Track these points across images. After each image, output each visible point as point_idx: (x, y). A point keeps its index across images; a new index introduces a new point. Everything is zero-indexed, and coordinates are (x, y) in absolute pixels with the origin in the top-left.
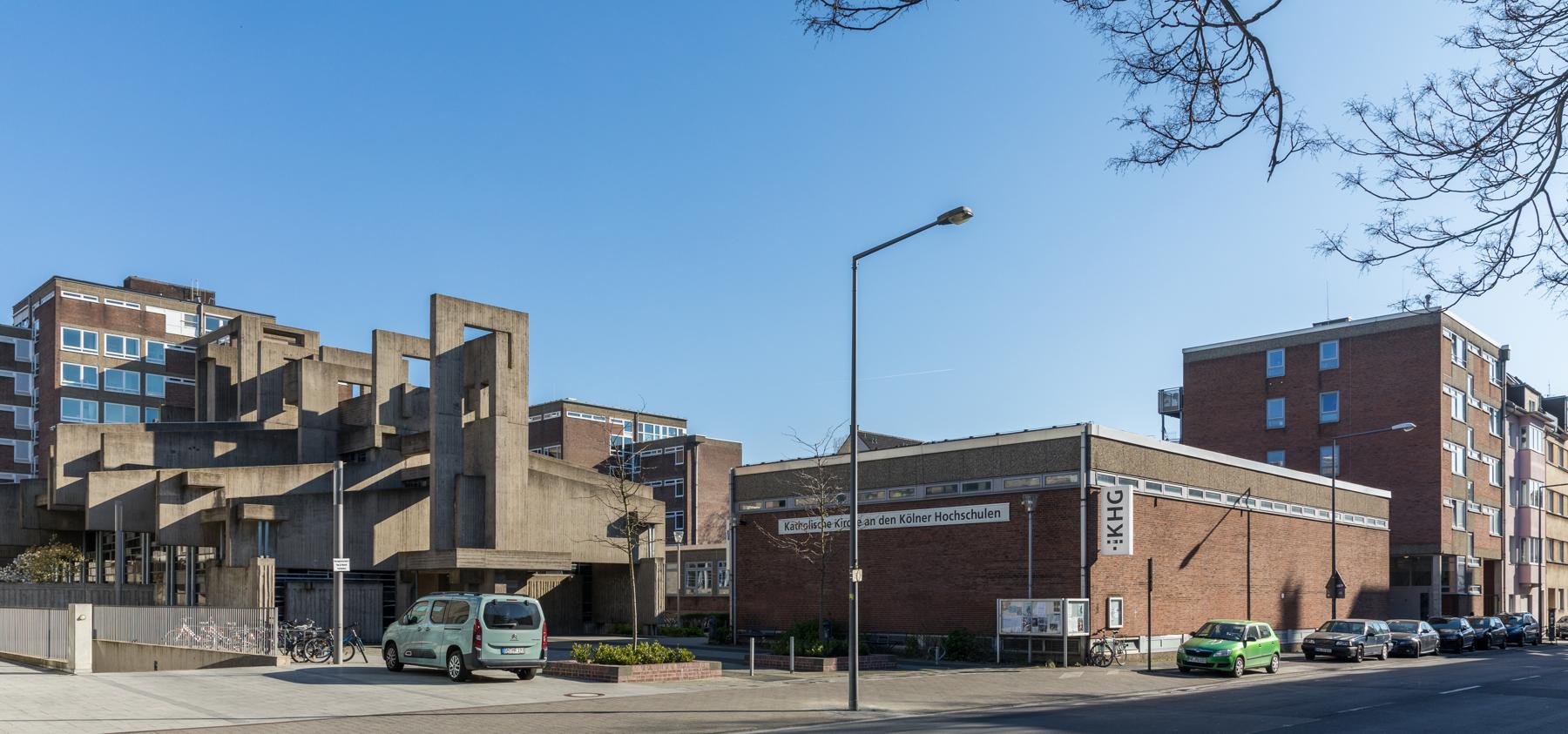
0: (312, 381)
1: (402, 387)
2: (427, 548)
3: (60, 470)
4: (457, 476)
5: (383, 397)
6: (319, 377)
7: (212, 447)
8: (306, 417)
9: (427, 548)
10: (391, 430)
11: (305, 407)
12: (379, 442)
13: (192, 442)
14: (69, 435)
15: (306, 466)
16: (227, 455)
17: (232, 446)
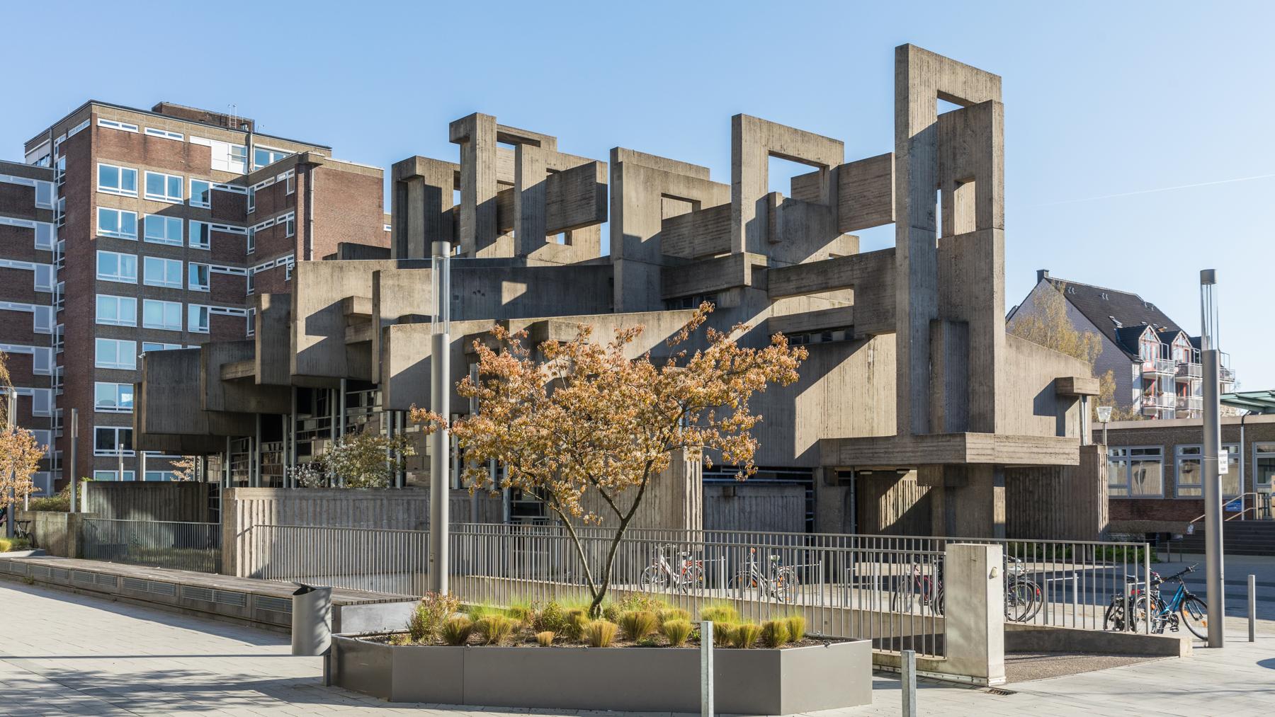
0: (633, 194)
1: (769, 198)
2: (893, 431)
3: (301, 325)
4: (933, 322)
5: (749, 213)
6: (641, 188)
7: (499, 291)
8: (622, 242)
9: (893, 431)
10: (761, 260)
11: (628, 229)
12: (748, 280)
13: (476, 284)
14: (311, 277)
15: (666, 315)
16: (514, 302)
17: (521, 288)
